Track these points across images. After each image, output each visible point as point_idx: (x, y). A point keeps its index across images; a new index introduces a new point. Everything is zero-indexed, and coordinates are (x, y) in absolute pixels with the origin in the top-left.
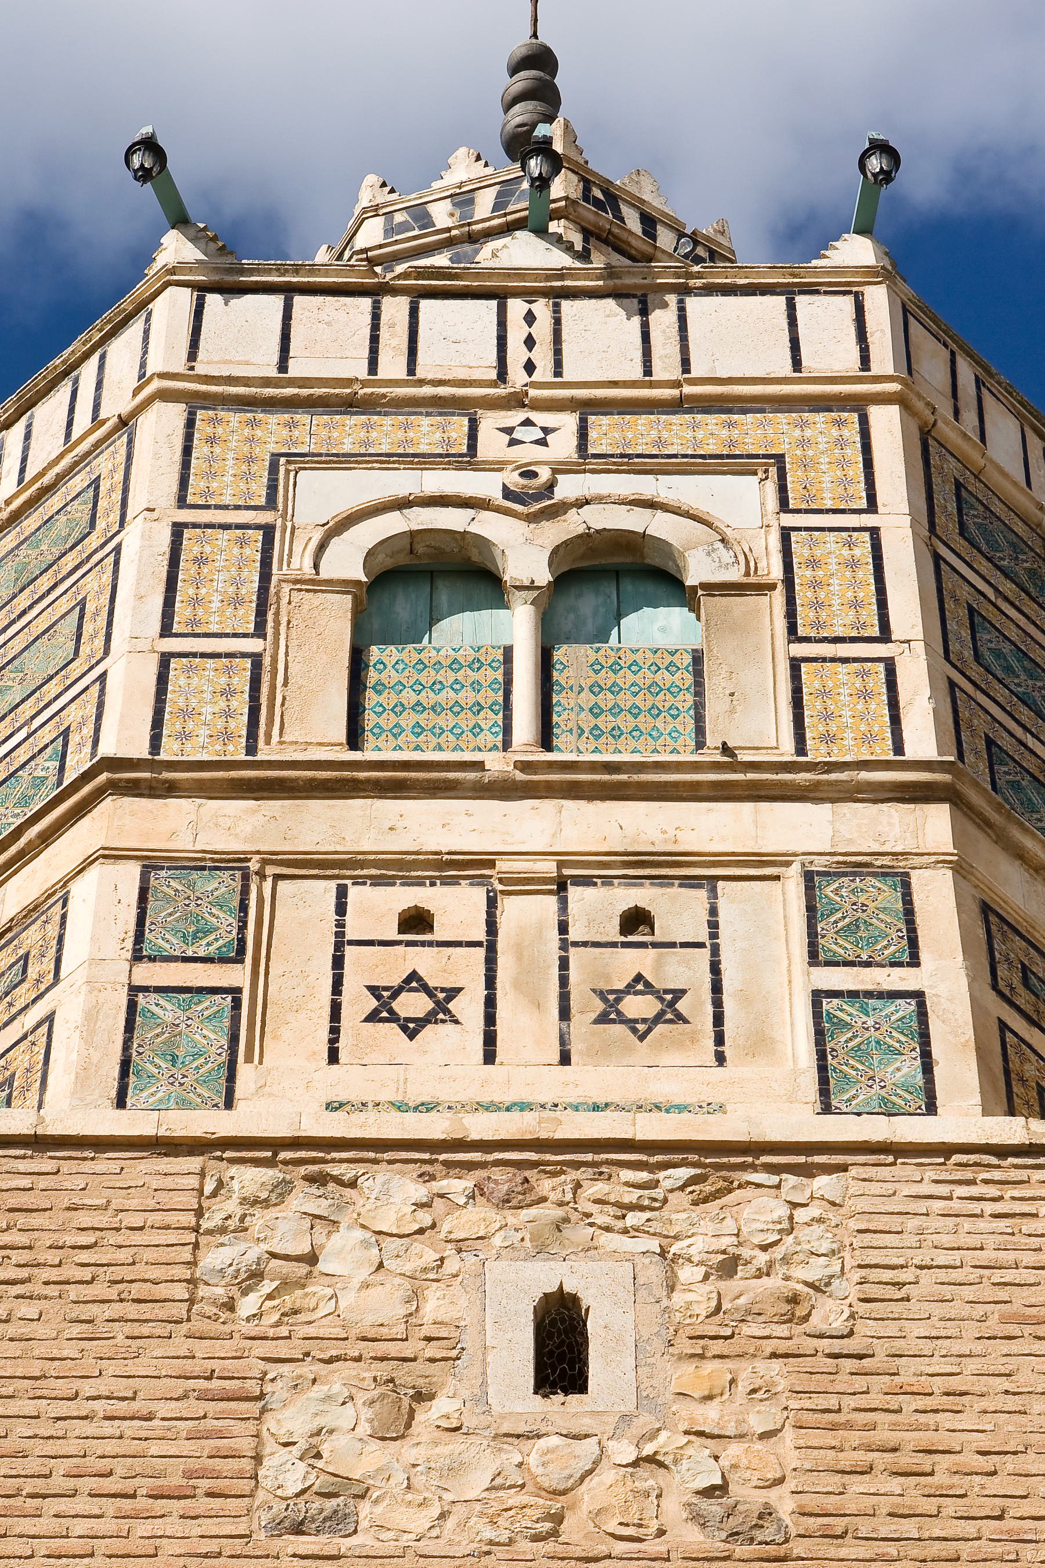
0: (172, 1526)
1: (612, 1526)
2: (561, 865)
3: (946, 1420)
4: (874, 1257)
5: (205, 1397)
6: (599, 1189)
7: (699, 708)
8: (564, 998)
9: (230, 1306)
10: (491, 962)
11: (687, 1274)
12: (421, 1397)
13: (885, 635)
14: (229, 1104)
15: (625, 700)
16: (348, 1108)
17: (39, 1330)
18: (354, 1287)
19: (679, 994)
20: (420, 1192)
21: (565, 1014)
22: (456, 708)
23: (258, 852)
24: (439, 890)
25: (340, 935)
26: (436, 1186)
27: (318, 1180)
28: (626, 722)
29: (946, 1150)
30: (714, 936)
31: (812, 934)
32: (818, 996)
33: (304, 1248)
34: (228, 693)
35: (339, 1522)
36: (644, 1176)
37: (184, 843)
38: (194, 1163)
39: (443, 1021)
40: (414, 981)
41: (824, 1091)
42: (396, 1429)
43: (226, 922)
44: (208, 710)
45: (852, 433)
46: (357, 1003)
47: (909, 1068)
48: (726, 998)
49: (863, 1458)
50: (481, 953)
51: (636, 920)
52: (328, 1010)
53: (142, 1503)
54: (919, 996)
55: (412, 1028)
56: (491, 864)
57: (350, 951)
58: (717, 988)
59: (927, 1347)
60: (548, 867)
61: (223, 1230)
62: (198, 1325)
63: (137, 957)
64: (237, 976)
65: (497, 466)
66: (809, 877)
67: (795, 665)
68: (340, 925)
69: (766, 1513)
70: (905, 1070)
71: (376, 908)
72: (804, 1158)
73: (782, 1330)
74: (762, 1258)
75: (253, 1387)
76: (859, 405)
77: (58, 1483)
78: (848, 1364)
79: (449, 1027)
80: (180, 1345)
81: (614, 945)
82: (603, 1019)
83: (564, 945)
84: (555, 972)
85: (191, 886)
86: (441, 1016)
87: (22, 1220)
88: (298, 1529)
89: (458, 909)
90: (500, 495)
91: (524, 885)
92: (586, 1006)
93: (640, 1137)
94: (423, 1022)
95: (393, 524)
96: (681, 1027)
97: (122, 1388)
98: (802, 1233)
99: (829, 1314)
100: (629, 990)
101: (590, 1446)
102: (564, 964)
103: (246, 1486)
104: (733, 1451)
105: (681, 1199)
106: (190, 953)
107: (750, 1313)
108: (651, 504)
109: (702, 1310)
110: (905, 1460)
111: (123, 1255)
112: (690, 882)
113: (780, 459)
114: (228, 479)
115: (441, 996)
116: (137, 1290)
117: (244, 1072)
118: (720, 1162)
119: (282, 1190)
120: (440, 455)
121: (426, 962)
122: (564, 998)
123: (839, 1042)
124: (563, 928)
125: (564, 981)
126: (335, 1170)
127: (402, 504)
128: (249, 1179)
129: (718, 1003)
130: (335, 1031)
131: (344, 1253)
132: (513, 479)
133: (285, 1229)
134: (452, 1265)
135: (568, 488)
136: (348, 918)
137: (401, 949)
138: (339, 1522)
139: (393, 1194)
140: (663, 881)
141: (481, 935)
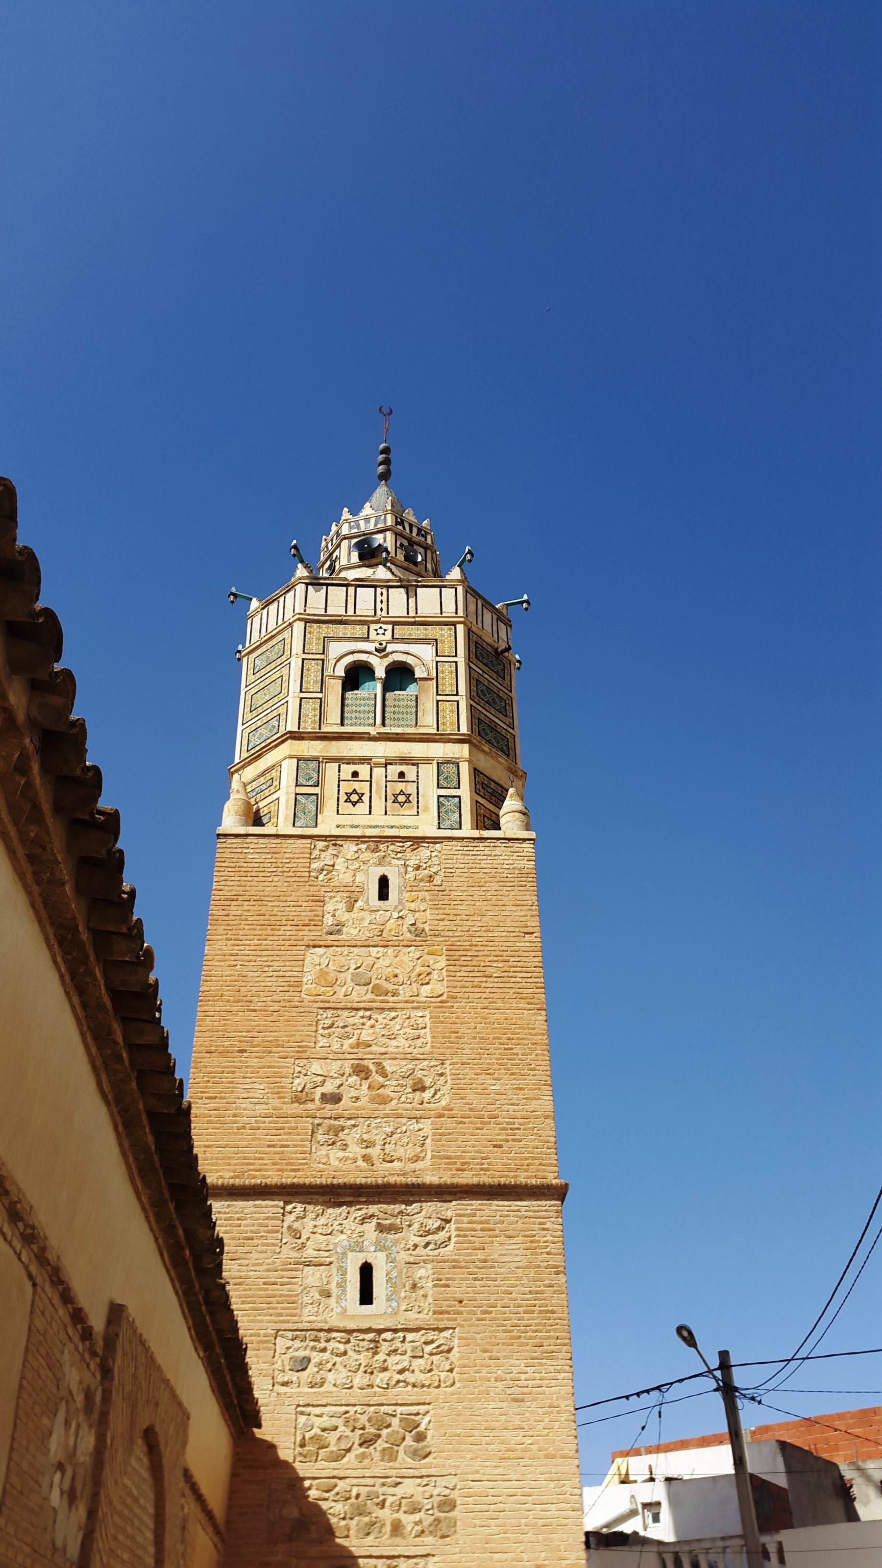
0: (306, 933)
1: (393, 933)
3: (460, 907)
4: (447, 866)
5: (313, 901)
6: (392, 847)
7: (417, 711)
8: (386, 796)
9: (317, 878)
10: (371, 786)
11: (410, 869)
12: (356, 901)
13: (457, 695)
14: (316, 826)
15: (401, 710)
17: (279, 884)
18: (341, 875)
19: (410, 795)
20: (355, 849)
21: (386, 801)
22: (364, 712)
24: (360, 766)
26: (359, 846)
27: (335, 845)
28: (401, 716)
29: (463, 838)
31: (438, 780)
32: (439, 796)
33: (332, 863)
34: (315, 709)
35: (339, 932)
36: (401, 844)
37: (306, 754)
38: (309, 841)
42: (350, 909)
43: (315, 775)
45: (453, 633)
46: (343, 797)
49: (442, 917)
53: (300, 927)
54: (459, 797)
55: (354, 804)
59: (456, 889)
60: (383, 760)
61: (315, 858)
62: (311, 883)
63: (297, 785)
64: (317, 790)
65: (373, 641)
66: (438, 763)
67: (438, 702)
69: (423, 930)
72: (435, 840)
73: (428, 884)
74: (425, 866)
75: (322, 899)
76: (454, 624)
77: (284, 922)
78: (441, 893)
80: (307, 888)
82: (394, 802)
83: (386, 781)
87: (275, 856)
88: (331, 934)
89: (364, 771)
91: (378, 765)
92: (391, 798)
94: (356, 802)
97: (295, 899)
98: (433, 859)
99: (438, 880)
100: (399, 794)
101: (388, 914)
103: (321, 923)
104: (418, 914)
105: (409, 850)
107: (422, 880)
109: (412, 879)
110: (451, 917)
111: (295, 865)
112: (413, 764)
113: (436, 640)
116: (298, 874)
118: (418, 841)
119: (327, 847)
121: (356, 785)
122: (386, 796)
123: (442, 810)
126: (338, 842)
127: (353, 653)
128: (321, 844)
131: (340, 864)
132: (378, 646)
133: (327, 858)
134: (362, 868)
135: (389, 649)
138: (339, 932)
139: (350, 848)
140: (407, 764)
141: (369, 779)
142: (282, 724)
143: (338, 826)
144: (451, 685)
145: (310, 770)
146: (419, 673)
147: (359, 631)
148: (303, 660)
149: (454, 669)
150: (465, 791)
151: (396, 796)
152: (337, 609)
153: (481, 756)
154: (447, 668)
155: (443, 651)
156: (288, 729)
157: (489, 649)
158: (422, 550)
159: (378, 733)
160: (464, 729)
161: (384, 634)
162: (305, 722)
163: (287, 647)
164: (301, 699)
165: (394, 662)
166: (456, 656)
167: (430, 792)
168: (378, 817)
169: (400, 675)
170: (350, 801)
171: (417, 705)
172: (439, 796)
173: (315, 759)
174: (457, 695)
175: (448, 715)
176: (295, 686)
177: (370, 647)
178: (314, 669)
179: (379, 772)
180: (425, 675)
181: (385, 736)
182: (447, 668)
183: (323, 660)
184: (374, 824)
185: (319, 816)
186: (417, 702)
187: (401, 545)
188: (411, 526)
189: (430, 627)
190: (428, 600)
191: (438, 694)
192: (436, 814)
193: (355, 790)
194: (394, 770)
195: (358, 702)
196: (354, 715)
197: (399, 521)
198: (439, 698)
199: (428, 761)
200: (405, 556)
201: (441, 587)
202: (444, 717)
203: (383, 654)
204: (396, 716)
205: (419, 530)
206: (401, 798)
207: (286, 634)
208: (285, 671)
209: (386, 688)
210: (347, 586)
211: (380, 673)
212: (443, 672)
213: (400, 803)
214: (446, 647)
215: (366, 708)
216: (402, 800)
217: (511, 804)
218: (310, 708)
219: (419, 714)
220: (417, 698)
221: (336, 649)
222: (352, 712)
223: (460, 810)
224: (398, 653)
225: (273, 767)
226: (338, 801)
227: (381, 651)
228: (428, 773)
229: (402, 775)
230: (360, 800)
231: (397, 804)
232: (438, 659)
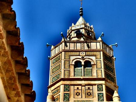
13: (101, 68)
22: (79, 73)
28: (88, 74)
31: (98, 89)
32: (98, 93)
34: (68, 73)
37: (66, 83)
40: (78, 92)
41: (98, 100)
46: (75, 94)
47: (102, 98)
50: (81, 90)
51: (89, 88)
54: (103, 93)
55: (78, 95)
60: (84, 85)
64: (69, 92)
65: (81, 56)
67: (97, 70)
76: (100, 51)
91: (83, 86)
94: (79, 95)
95: (76, 60)
121: (78, 91)
127: (76, 59)
135: (85, 57)
142: (60, 76)
144: (100, 66)
145: (67, 88)
146: (92, 63)
147: (77, 53)
148: (65, 61)
149: (100, 62)
150: (104, 92)
151: (88, 93)
152: (72, 48)
153: (108, 83)
155: (98, 58)
156: (62, 77)
157: (108, 57)
158: (91, 33)
160: (103, 77)
162: (66, 76)
163: (61, 58)
164: (64, 70)
165: (86, 61)
167: (96, 92)
169: (88, 64)
172: (98, 93)
174: (101, 68)
175: (100, 74)
176: (63, 67)
177: (80, 57)
178: (67, 62)
179: (83, 88)
180: (93, 64)
183: (69, 61)
185: (70, 99)
187: (86, 32)
188: (88, 27)
190: (93, 45)
191: (97, 68)
192: (97, 98)
194: (87, 87)
195: (78, 71)
196: (77, 74)
197: (86, 26)
198: (97, 69)
199: (95, 85)
200: (87, 34)
201: (96, 42)
204: (87, 74)
205: (90, 28)
206: (89, 94)
207: (60, 54)
208: (60, 63)
209: (84, 68)
210: (74, 43)
211: (83, 63)
213: (89, 95)
214: (98, 57)
215: (80, 72)
217: (116, 94)
218: (66, 72)
219: (93, 73)
221: (72, 58)
222: (76, 73)
224: (87, 58)
225: (58, 87)
227: (83, 58)
228: (95, 88)
230: (79, 95)
232: (96, 60)
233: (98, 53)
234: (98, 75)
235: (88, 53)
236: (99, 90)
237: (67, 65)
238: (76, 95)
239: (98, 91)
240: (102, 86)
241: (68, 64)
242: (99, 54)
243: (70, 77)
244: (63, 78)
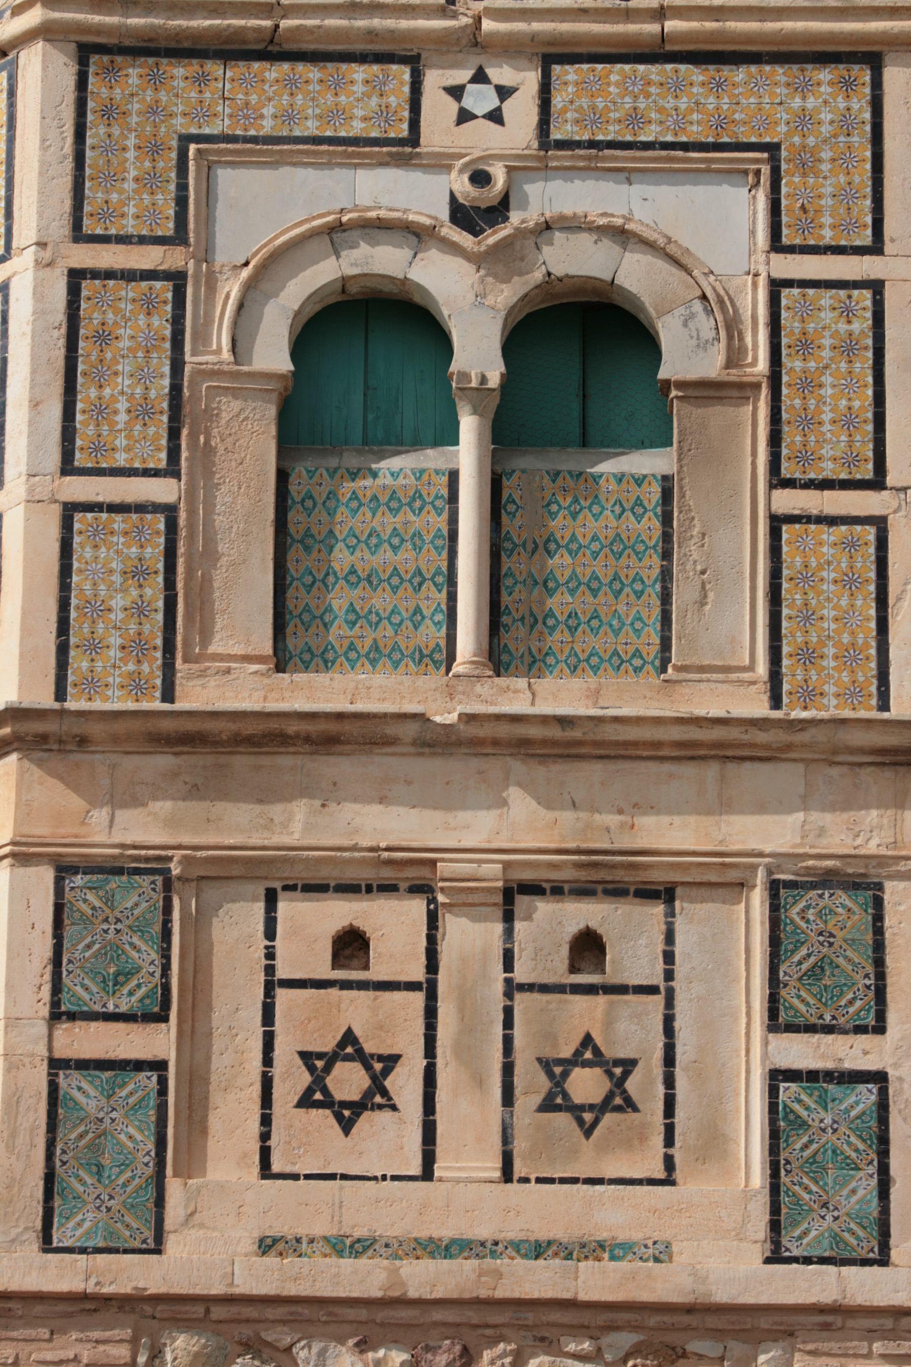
2: (507, 865)
7: (666, 575)
10: (431, 1013)
16: (281, 1246)
19: (629, 1065)
23: (179, 847)
25: (270, 970)
30: (669, 976)
32: (778, 1077)
39: (380, 1107)
43: (146, 955)
44: (118, 602)
46: (291, 1080)
48: (678, 1072)
50: (418, 999)
52: (257, 1089)
54: (880, 1078)
55: (348, 1115)
56: (433, 863)
57: (282, 995)
58: (669, 1060)
60: (492, 871)
63: (57, 1015)
64: (159, 1042)
65: (441, 163)
66: (774, 888)
67: (776, 522)
68: (270, 955)
70: (861, 1193)
71: (311, 926)
79: (385, 1116)
81: (559, 989)
82: (548, 1106)
83: (511, 988)
84: (498, 1030)
85: (109, 900)
86: (378, 1099)
89: (393, 928)
90: (444, 213)
91: (468, 901)
92: (531, 1083)
93: (583, 1296)
94: (359, 1107)
96: (632, 1116)
100: (576, 1060)
102: (508, 1013)
106: (111, 1008)
108: (622, 235)
112: (647, 893)
113: (773, 149)
114: (129, 186)
115: (378, 1066)
117: (174, 1188)
120: (375, 142)
122: (508, 1069)
123: (795, 1147)
124: (508, 965)
125: (508, 1042)
126: (269, 1336)
129: (669, 1082)
130: (266, 1120)
136: (279, 943)
137: (334, 992)
140: (616, 892)
141: (418, 973)
143: (267, 1245)
146: (686, 351)
149: (862, 324)
151: (556, 1070)
154: (828, 321)
159: (469, 718)
161: (495, 116)
162: (94, 647)
164: (70, 510)
166: (876, 248)
168: (469, 1196)
169: (585, 350)
170: (328, 1103)
171: (667, 537)
172: (778, 1077)
173: (150, 867)
178: (131, 324)
179: (470, 938)
180: (711, 365)
181: (503, 731)
182: (828, 321)
183: (178, 279)
184: (446, 1232)
186: (667, 519)
189: (740, 74)
192: (758, 1178)
193: (349, 1037)
194: (550, 925)
198: (787, 501)
202: (808, 616)
203: (493, 237)
211: (478, 352)
212: (806, 346)
213: (576, 1110)
214: (827, 194)
215: (405, 558)
216: (590, 1096)
220: (667, 496)
223: (884, 1153)
226: (266, 1099)
228: (728, 945)
229: (588, 947)
230: (377, 1097)
231: (563, 1120)
233: (827, 97)
234: (809, 656)
235: (594, 98)
236: (799, 1001)
237: (128, 381)
238: (306, 1102)
239: (777, 1020)
240: (862, 919)
241: (140, 376)
242: (845, 124)
243: (199, 694)
244: (45, 699)
